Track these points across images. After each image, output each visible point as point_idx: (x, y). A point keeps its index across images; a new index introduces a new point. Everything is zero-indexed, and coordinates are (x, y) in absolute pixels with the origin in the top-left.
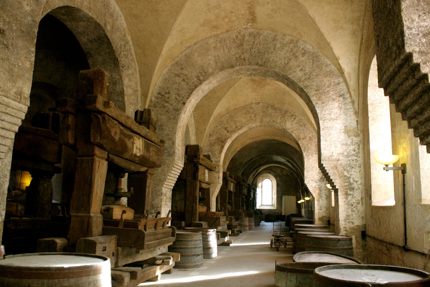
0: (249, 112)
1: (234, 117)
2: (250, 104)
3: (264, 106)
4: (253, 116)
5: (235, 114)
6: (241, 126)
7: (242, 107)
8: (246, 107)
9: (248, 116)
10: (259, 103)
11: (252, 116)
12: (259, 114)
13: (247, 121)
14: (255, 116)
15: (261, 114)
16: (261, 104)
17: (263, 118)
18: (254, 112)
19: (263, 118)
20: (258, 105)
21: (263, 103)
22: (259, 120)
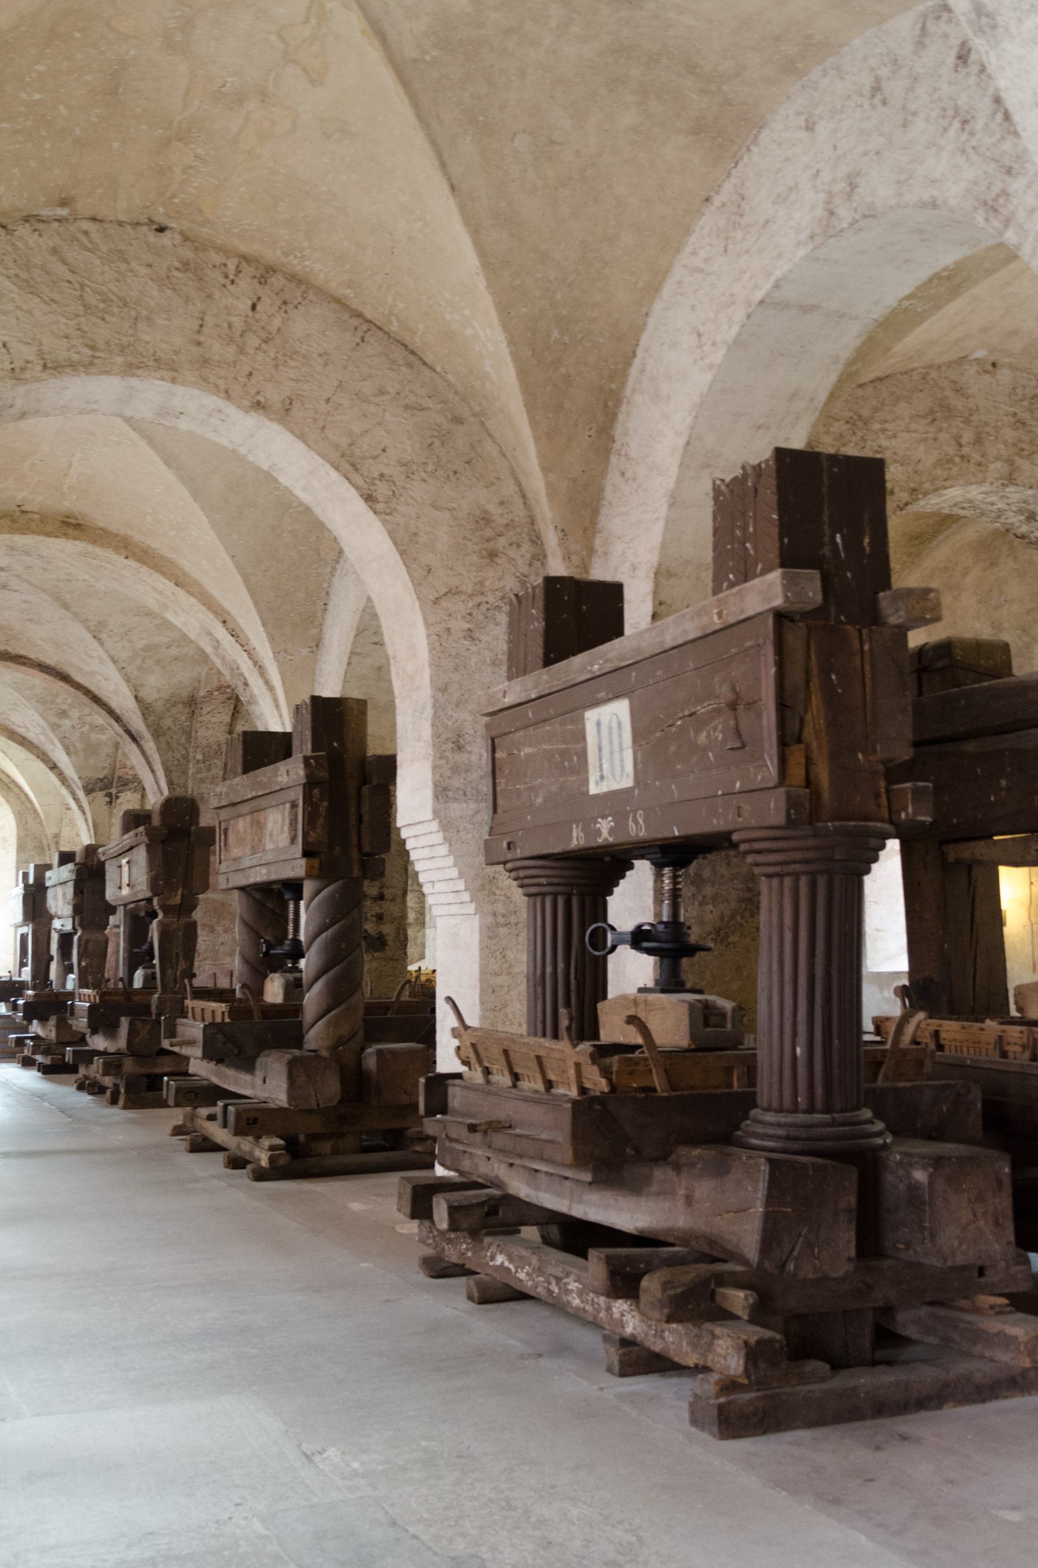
0: (948, 411)
1: (877, 426)
2: (949, 365)
3: (1019, 391)
4: (967, 437)
5: (876, 410)
6: (914, 490)
7: (915, 376)
8: (934, 374)
9: (944, 436)
10: (994, 365)
11: (964, 440)
12: (997, 429)
13: (938, 463)
14: (978, 441)
15: (1009, 434)
16: (1004, 376)
17: (1019, 461)
18: (975, 418)
19: (1019, 461)
20: (987, 378)
21: (1011, 367)
22: (999, 465)
